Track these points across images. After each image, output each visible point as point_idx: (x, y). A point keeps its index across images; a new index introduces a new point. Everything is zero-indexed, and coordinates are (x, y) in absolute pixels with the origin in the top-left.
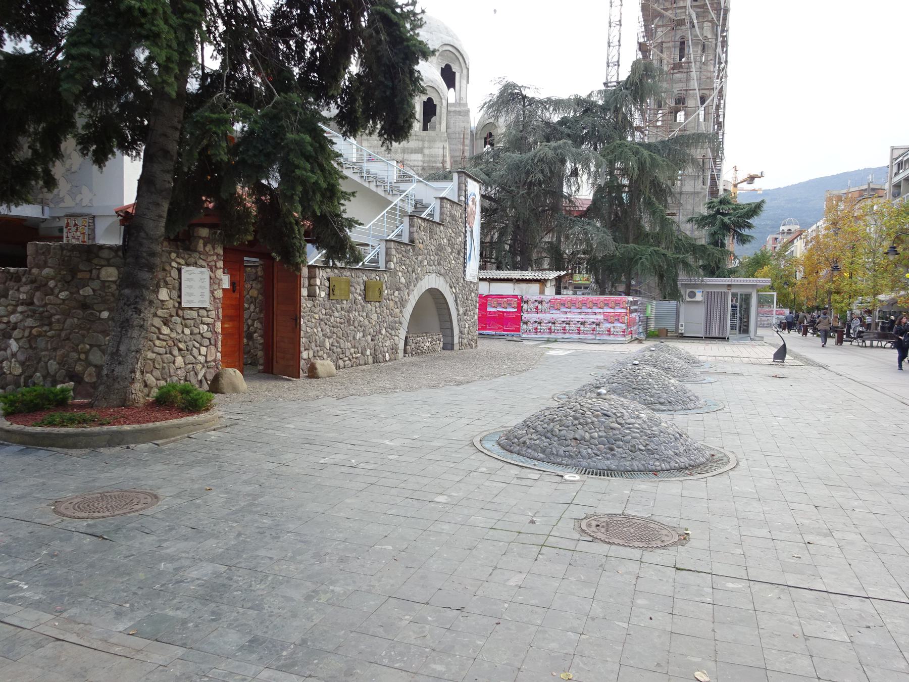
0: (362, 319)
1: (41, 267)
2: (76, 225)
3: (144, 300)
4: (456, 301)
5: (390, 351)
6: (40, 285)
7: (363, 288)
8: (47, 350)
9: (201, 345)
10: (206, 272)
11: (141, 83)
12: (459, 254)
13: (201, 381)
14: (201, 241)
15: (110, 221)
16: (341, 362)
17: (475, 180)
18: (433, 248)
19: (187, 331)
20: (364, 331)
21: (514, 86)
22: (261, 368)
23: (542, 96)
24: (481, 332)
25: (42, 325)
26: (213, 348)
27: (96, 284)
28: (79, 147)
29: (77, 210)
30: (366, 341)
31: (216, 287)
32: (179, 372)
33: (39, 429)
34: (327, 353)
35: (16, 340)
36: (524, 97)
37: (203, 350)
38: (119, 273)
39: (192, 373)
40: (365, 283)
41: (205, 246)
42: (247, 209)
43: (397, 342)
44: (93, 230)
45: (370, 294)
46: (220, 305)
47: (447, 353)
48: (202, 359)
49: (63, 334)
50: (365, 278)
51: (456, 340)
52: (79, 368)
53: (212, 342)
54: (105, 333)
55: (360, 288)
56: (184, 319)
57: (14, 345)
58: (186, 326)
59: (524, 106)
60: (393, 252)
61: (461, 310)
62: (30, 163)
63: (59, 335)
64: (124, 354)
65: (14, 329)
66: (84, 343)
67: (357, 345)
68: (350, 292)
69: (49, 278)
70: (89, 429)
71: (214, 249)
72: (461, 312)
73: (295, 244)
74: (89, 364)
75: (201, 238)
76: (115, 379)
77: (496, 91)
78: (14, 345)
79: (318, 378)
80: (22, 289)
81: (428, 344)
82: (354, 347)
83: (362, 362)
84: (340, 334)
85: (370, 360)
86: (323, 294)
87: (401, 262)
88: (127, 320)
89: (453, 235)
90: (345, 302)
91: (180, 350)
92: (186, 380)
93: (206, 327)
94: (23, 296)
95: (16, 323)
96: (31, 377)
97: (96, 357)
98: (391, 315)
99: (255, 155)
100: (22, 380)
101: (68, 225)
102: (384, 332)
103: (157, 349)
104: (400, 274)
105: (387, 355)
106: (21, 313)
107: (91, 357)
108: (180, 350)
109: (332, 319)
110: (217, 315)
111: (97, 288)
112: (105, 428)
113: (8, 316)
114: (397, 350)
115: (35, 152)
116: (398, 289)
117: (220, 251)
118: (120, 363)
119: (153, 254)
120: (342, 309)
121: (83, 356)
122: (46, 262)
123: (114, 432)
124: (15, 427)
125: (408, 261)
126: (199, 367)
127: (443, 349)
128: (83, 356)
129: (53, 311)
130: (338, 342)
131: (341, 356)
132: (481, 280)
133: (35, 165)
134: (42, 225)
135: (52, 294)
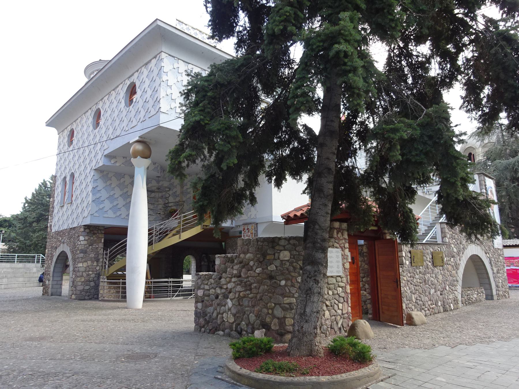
0: (432, 279)
1: (245, 253)
2: (248, 229)
3: (320, 273)
4: (491, 263)
5: (453, 302)
6: (244, 265)
7: (431, 257)
8: (248, 306)
9: (339, 302)
10: (339, 250)
11: (301, 135)
13: (340, 329)
14: (335, 231)
15: (265, 225)
17: (490, 178)
20: (435, 288)
22: (370, 316)
24: (510, 285)
25: (246, 290)
26: (345, 303)
27: (277, 263)
28: (267, 178)
29: (248, 221)
30: (437, 295)
31: (345, 261)
32: (327, 322)
33: (261, 376)
34: (414, 305)
35: (231, 300)
37: (340, 305)
38: (291, 255)
39: (335, 322)
40: (432, 254)
41: (337, 234)
42: (369, 207)
43: (457, 295)
44: (257, 231)
45: (437, 261)
46: (348, 274)
47: (489, 302)
48: (340, 312)
49: (258, 297)
50: (432, 250)
52: (268, 320)
53: (345, 300)
55: (429, 257)
56: (328, 284)
57: (230, 303)
58: (330, 289)
59: (502, 130)
60: (447, 231)
61: (495, 270)
62: (243, 189)
63: (256, 297)
64: (309, 315)
65: (230, 292)
66: (271, 302)
67: (432, 299)
68: (423, 261)
69: (250, 260)
70: (296, 379)
71: (343, 235)
72: (495, 271)
73: (411, 227)
74: (274, 317)
75: (335, 228)
76: (304, 334)
78: (230, 303)
79: (415, 325)
80: (234, 267)
82: (430, 300)
83: (437, 311)
84: (421, 291)
85: (442, 310)
86: (407, 262)
87: (452, 238)
88: (310, 289)
90: (421, 267)
91: (327, 306)
92: (331, 328)
93: (341, 289)
94: (235, 272)
95: (231, 289)
96: (239, 324)
97: (279, 312)
98: (451, 275)
99: (417, 155)
100: (234, 326)
101: (244, 229)
104: (453, 246)
105: (452, 305)
106: (234, 282)
107: (275, 312)
108: (327, 306)
109: (415, 280)
110: (347, 280)
111: (278, 265)
112: (308, 378)
113: (226, 284)
114: (457, 301)
115: (246, 183)
116: (453, 257)
117: (346, 236)
118: (306, 322)
119: (324, 240)
120: (420, 272)
121: (270, 311)
122: (248, 250)
123: (314, 383)
124: (244, 371)
125: (456, 236)
126: (339, 318)
127: (487, 299)
128: (270, 311)
129: (252, 281)
130: (420, 297)
131: (423, 307)
132: (505, 247)
133: (245, 190)
134: (231, 231)
135: (252, 270)
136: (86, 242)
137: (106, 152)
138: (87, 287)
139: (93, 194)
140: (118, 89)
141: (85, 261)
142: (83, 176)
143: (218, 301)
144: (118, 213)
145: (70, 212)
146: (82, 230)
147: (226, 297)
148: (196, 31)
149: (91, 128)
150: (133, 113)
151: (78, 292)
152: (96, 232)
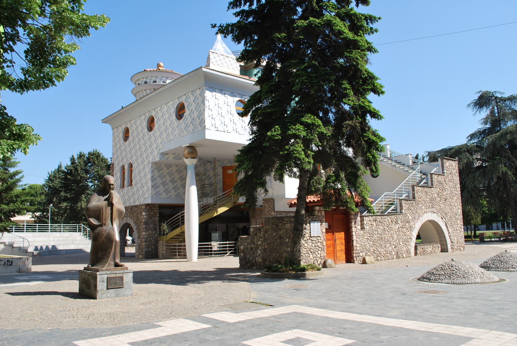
4: (446, 225)
12: (445, 200)
16: (379, 258)
18: (427, 199)
19: (313, 245)
21: (487, 93)
23: (506, 95)
36: (496, 98)
37: (319, 252)
43: (409, 248)
48: (319, 256)
51: (449, 247)
54: (287, 247)
60: (403, 205)
77: (476, 97)
81: (430, 249)
86: (368, 228)
89: (440, 191)
102: (401, 243)
103: (304, 252)
105: (404, 255)
125: (412, 208)
127: (441, 251)
136: (147, 217)
137: (161, 151)
138: (150, 250)
139: (152, 181)
140: (169, 104)
141: (148, 231)
142: (141, 167)
143: (252, 251)
144: (169, 194)
145: (131, 194)
146: (144, 207)
147: (257, 248)
148: (223, 57)
149: (146, 130)
150: (183, 126)
151: (144, 253)
152: (153, 208)
